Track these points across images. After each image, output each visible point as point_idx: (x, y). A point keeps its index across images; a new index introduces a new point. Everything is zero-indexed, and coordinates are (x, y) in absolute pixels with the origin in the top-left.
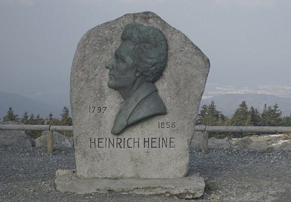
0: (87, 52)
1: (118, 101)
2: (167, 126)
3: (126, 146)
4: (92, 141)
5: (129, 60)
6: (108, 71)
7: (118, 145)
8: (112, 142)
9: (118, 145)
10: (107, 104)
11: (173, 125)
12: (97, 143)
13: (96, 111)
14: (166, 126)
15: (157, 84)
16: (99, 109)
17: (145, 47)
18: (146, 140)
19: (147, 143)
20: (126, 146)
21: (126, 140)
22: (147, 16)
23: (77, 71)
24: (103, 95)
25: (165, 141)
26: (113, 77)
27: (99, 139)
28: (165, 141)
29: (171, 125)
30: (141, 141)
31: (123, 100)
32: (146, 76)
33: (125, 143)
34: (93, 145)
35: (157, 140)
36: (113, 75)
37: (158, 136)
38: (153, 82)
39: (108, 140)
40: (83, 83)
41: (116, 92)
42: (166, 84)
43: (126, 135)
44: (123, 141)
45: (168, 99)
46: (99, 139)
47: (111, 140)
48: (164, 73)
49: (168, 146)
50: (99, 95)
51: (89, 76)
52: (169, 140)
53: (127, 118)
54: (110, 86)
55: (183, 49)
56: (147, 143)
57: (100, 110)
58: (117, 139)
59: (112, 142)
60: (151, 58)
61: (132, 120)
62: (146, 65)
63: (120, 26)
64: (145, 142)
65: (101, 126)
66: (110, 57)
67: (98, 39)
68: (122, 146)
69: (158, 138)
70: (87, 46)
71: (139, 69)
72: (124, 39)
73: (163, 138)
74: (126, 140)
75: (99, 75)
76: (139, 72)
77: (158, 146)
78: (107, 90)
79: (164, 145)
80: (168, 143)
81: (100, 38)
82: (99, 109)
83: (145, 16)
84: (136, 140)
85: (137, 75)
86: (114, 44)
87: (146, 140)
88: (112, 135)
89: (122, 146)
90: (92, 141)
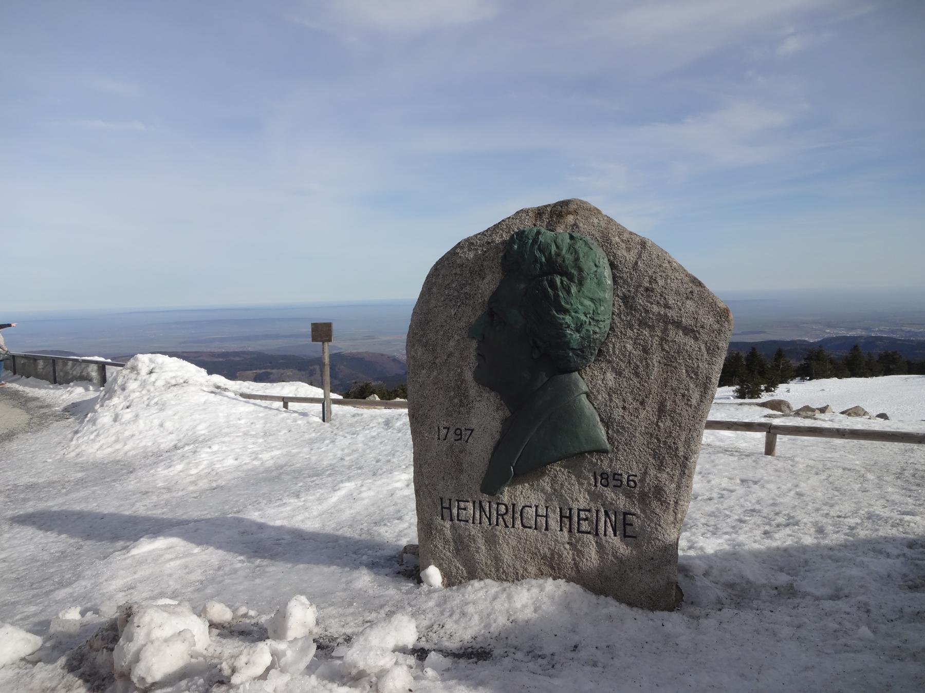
0: (433, 302)
1: (499, 415)
2: (615, 483)
3: (518, 522)
4: (444, 505)
9: (501, 519)
10: (474, 422)
12: (455, 511)
13: (451, 436)
16: (458, 432)
19: (566, 521)
20: (518, 522)
23: (414, 345)
24: (465, 401)
29: (625, 482)
33: (518, 515)
34: (446, 512)
39: (477, 505)
41: (493, 393)
50: (456, 401)
51: (436, 358)
57: (459, 434)
58: (498, 504)
64: (561, 517)
65: (461, 471)
67: (454, 272)
70: (434, 290)
73: (606, 513)
75: (457, 354)
78: (473, 390)
79: (610, 530)
80: (620, 525)
81: (458, 271)
82: (458, 432)
84: (542, 511)
86: (486, 281)
90: (444, 505)
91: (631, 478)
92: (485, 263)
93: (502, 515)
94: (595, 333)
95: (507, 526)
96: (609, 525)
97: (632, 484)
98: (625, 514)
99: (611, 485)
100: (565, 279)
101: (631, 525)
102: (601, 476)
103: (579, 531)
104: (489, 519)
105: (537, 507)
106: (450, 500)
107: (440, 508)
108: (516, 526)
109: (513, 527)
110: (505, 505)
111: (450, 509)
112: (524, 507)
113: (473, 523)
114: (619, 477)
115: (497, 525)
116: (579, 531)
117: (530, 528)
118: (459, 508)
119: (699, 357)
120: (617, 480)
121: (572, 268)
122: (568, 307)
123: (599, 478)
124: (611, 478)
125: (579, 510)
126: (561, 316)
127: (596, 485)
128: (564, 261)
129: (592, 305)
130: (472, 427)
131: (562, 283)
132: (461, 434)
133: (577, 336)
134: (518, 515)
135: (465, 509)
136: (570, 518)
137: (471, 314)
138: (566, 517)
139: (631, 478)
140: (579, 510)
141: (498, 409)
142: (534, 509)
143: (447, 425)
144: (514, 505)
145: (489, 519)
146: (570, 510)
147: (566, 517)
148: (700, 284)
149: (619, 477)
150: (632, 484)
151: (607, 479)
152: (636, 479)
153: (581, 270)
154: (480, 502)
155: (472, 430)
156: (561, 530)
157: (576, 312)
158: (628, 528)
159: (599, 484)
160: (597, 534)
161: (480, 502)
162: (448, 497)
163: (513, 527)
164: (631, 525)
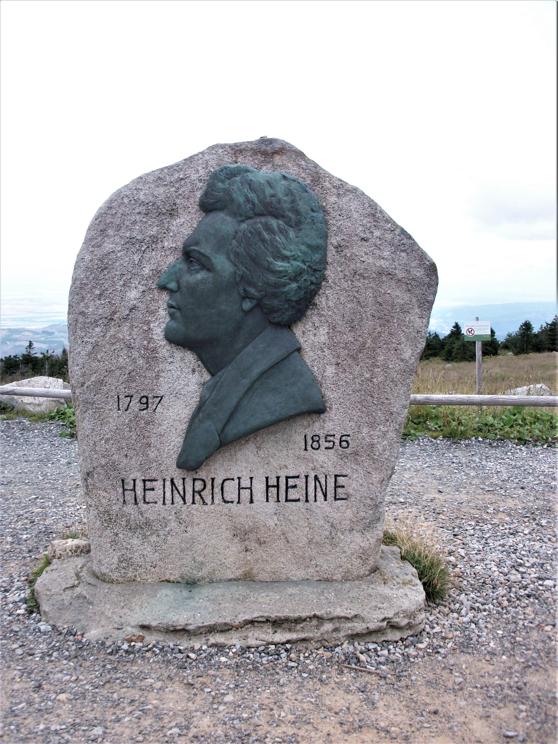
5: (222, 263)
6: (165, 296)
7: (197, 497)
8: (180, 488)
9: (197, 497)
11: (344, 441)
13: (135, 405)
14: (324, 444)
15: (298, 330)
17: (268, 228)
18: (272, 482)
19: (273, 491)
21: (218, 482)
22: (269, 150)
25: (323, 483)
26: (178, 314)
27: (144, 481)
28: (323, 483)
29: (337, 442)
30: (259, 487)
31: (207, 377)
32: (273, 310)
33: (217, 490)
35: (301, 482)
36: (179, 309)
37: (302, 470)
38: (289, 325)
39: (168, 483)
40: (98, 329)
42: (323, 330)
43: (218, 470)
44: (209, 486)
45: (330, 371)
46: (144, 481)
47: (179, 483)
48: (317, 300)
49: (329, 496)
52: (331, 481)
53: (220, 426)
54: (172, 338)
55: (368, 235)
56: (273, 491)
58: (194, 480)
59: (180, 488)
60: (285, 258)
61: (235, 431)
62: (272, 278)
63: (199, 176)
64: (268, 487)
66: (171, 259)
68: (208, 500)
69: (303, 476)
71: (252, 290)
72: (207, 206)
73: (316, 478)
74: (218, 482)
76: (251, 298)
77: (303, 498)
79: (320, 495)
82: (144, 400)
83: (263, 147)
84: (245, 483)
85: (247, 305)
87: (272, 482)
88: (179, 471)
89: (208, 500)
91: (344, 438)
92: (178, 201)
93: (199, 493)
94: (312, 283)
95: (204, 503)
96: (319, 489)
97: (344, 444)
98: (336, 476)
99: (322, 448)
100: (281, 222)
101: (343, 487)
102: (312, 438)
103: (287, 500)
104: (184, 499)
105: (239, 478)
106: (134, 480)
107: (120, 490)
108: (216, 501)
109: (213, 502)
110: (203, 481)
111: (134, 490)
112: (224, 480)
113: (164, 503)
114: (332, 438)
115: (193, 503)
116: (287, 500)
117: (232, 502)
118: (145, 490)
119: (411, 311)
120: (330, 441)
121: (289, 211)
122: (288, 253)
123: (310, 442)
124: (322, 441)
125: (287, 478)
126: (280, 264)
127: (306, 449)
128: (279, 203)
129: (310, 252)
130: (161, 393)
131: (279, 227)
132: (147, 403)
133: (294, 285)
134: (217, 490)
135: (153, 489)
136: (278, 486)
137: (165, 258)
138: (273, 486)
139: (344, 438)
140: (287, 478)
141: (194, 371)
142: (237, 481)
143: (128, 392)
144: (213, 480)
145: (184, 499)
146: (278, 478)
147: (273, 486)
148: (410, 238)
149: (332, 438)
150: (344, 444)
151: (318, 441)
152: (349, 439)
153: (297, 212)
154: (172, 481)
155: (162, 397)
156: (267, 501)
157: (294, 259)
158: (339, 490)
159: (309, 448)
160: (307, 501)
161: (172, 481)
162: (132, 476)
163: (213, 502)
164: (343, 487)
